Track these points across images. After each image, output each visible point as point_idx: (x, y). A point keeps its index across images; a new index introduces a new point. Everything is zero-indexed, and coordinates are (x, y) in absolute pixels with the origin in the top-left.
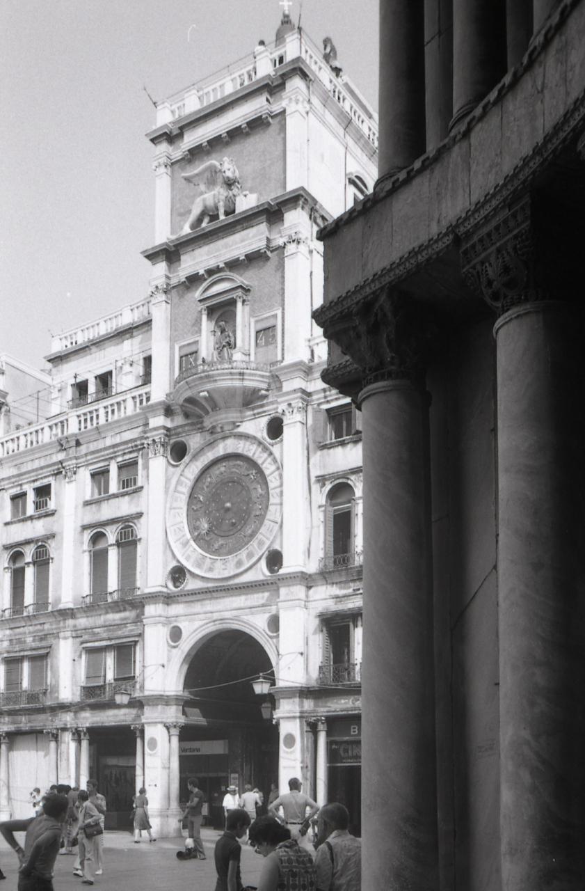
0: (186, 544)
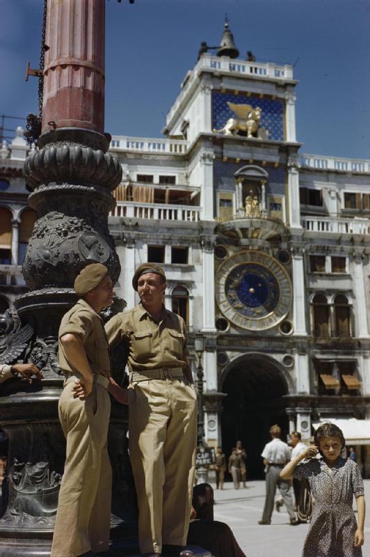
0: (224, 306)
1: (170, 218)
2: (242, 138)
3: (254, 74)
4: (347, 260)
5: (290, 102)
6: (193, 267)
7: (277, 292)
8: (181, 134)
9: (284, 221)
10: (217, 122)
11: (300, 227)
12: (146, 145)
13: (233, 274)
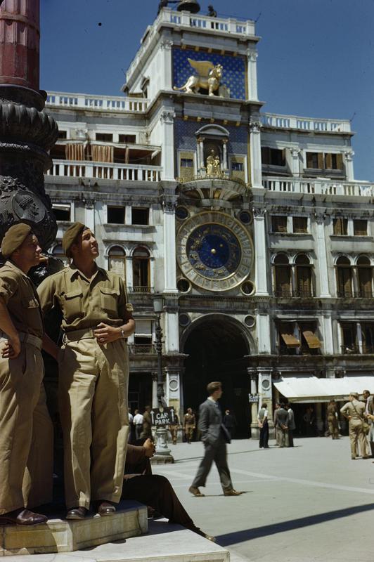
0: (186, 267)
1: (130, 178)
2: (203, 96)
3: (215, 29)
4: (309, 220)
5: (252, 59)
6: (154, 227)
7: (238, 252)
8: (141, 91)
9: (246, 182)
10: (177, 80)
11: (263, 188)
12: (105, 103)
13: (194, 235)
